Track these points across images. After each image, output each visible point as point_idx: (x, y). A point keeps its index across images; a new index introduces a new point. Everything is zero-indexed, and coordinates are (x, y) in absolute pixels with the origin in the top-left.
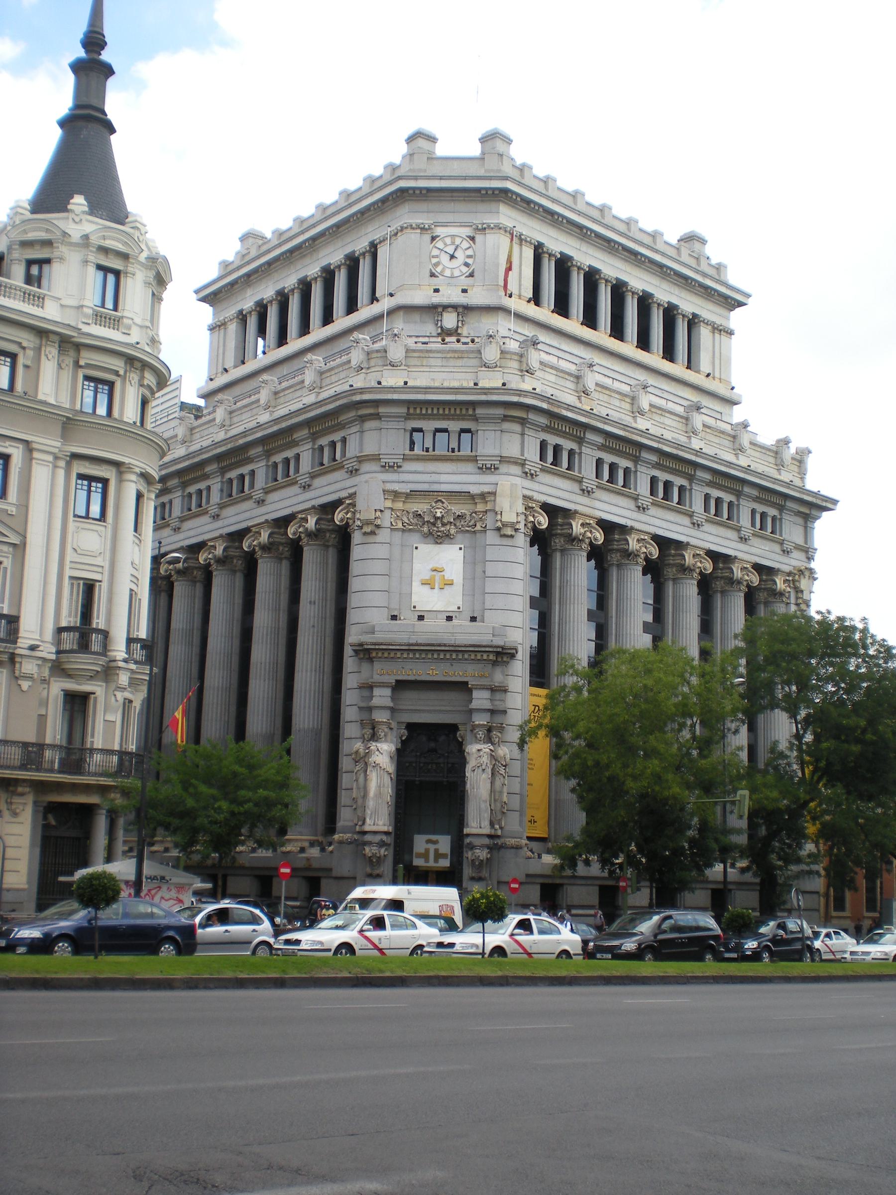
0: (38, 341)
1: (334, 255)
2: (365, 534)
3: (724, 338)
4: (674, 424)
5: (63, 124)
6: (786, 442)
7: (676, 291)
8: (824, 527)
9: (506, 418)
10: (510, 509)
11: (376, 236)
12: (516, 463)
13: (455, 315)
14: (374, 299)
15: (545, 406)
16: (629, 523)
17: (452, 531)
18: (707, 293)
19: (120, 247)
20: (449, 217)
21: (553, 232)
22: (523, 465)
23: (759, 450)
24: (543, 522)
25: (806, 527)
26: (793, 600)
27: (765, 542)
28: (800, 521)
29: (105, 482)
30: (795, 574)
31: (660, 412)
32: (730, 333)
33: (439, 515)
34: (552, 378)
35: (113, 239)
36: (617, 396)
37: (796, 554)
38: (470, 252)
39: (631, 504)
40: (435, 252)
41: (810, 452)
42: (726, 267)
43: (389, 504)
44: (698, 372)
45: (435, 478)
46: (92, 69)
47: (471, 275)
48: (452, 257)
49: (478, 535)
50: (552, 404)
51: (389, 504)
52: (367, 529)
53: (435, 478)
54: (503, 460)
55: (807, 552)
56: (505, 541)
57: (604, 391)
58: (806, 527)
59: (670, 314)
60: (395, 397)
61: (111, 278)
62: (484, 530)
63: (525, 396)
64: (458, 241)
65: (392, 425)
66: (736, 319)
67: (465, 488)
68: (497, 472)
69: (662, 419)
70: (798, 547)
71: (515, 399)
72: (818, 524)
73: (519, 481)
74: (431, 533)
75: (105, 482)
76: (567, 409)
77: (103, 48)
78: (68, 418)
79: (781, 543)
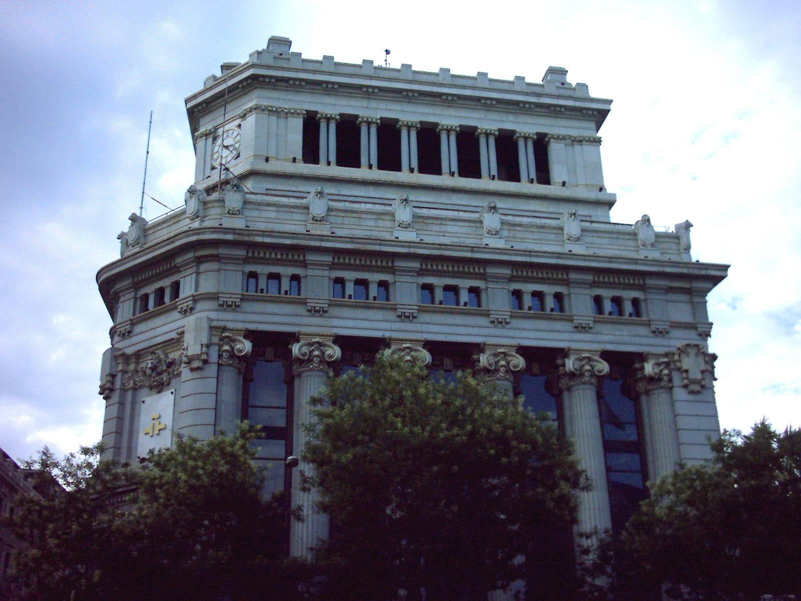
3: (588, 148)
4: (464, 230)
7: (505, 117)
8: (717, 301)
9: (199, 260)
15: (230, 237)
16: (387, 335)
23: (606, 235)
27: (621, 327)
30: (674, 354)
31: (439, 222)
34: (273, 215)
36: (369, 216)
37: (676, 333)
43: (120, 367)
50: (239, 234)
57: (350, 215)
68: (193, 312)
69: (443, 228)
73: (213, 315)
76: (263, 236)
79: (648, 324)
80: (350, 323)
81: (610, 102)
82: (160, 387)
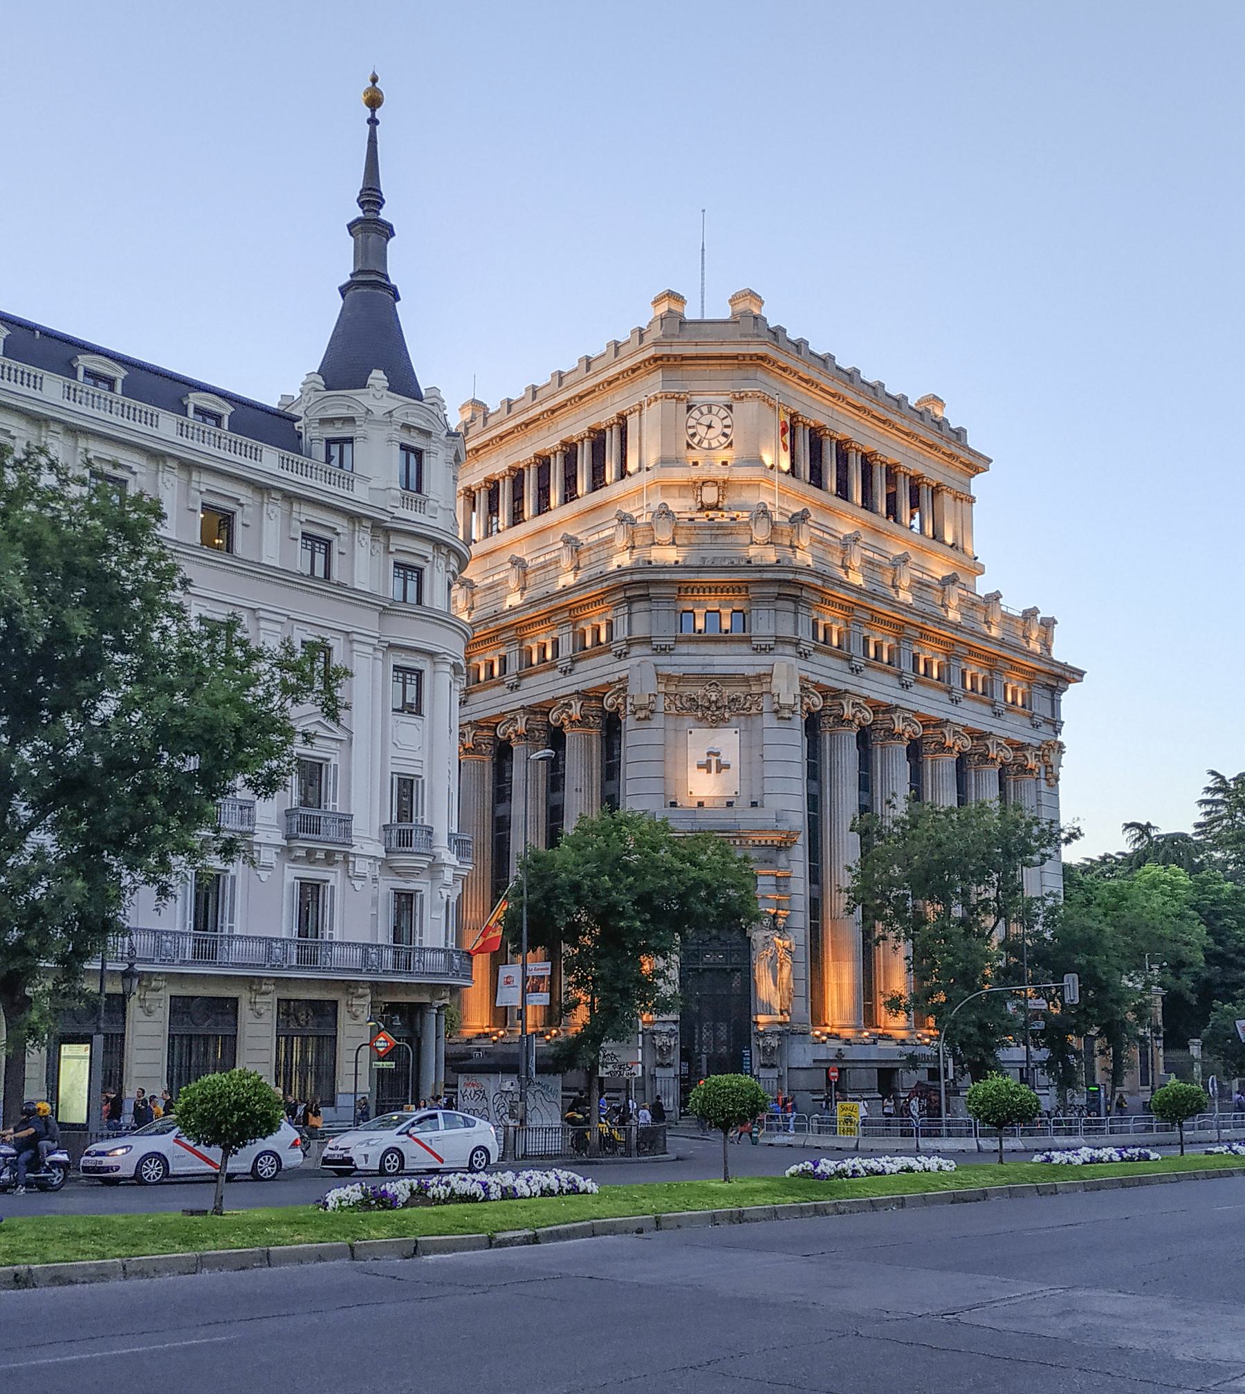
0: (351, 527)
1: (575, 426)
2: (639, 719)
5: (343, 290)
6: (1033, 612)
8: (1071, 700)
9: (780, 597)
10: (786, 689)
11: (623, 407)
12: (790, 643)
13: (715, 489)
14: (623, 473)
17: (727, 716)
19: (423, 425)
20: (705, 385)
22: (797, 644)
24: (818, 702)
25: (1053, 700)
26: (1043, 775)
28: (1047, 694)
29: (419, 674)
33: (714, 698)
35: (413, 415)
37: (1045, 728)
38: (727, 422)
39: (894, 681)
40: (692, 422)
41: (1055, 622)
42: (965, 431)
43: (662, 688)
45: (708, 660)
46: (371, 229)
47: (731, 444)
48: (709, 427)
49: (754, 718)
51: (662, 688)
52: (642, 714)
53: (708, 660)
54: (780, 640)
55: (1054, 725)
56: (783, 724)
58: (1053, 700)
60: (667, 577)
61: (412, 456)
62: (761, 712)
63: (800, 573)
64: (715, 409)
65: (662, 606)
67: (740, 670)
70: (1047, 721)
71: (791, 576)
72: (1064, 696)
74: (704, 718)
75: (419, 674)
77: (381, 207)
78: (384, 608)
80: (875, 686)
82: (718, 722)
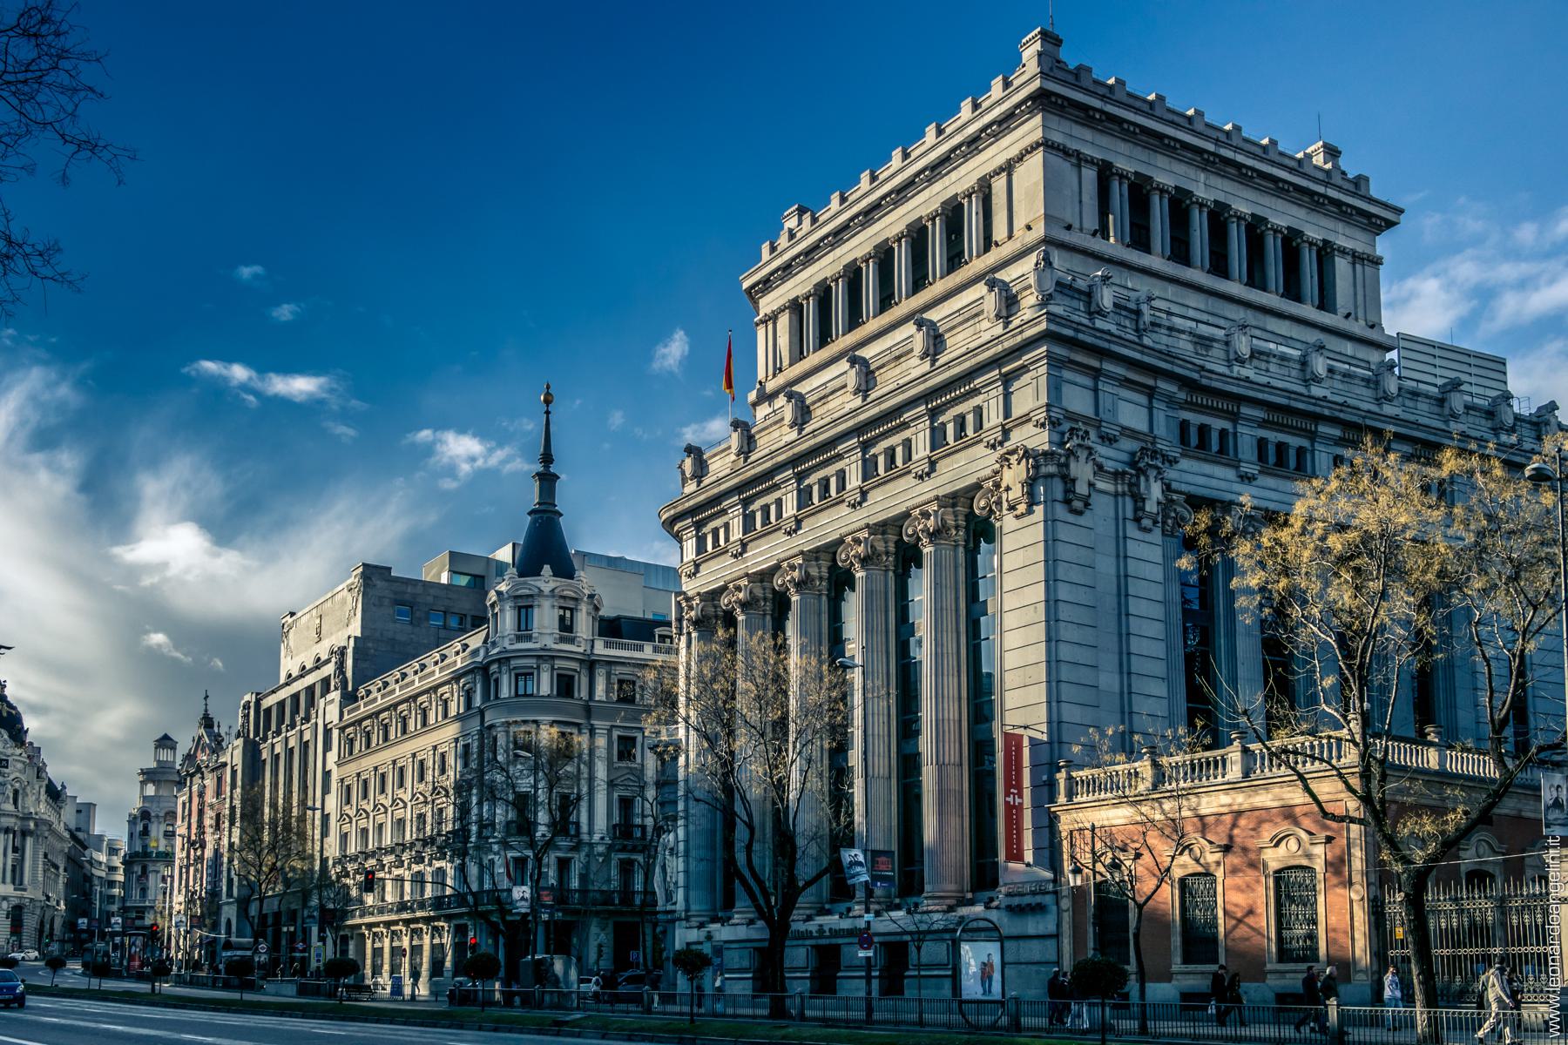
18: (1342, 212)
21: (1123, 147)
32: (1377, 262)
42: (1367, 179)
44: (1335, 313)
59: (1291, 241)
66: (1383, 246)
81: (1402, 211)
